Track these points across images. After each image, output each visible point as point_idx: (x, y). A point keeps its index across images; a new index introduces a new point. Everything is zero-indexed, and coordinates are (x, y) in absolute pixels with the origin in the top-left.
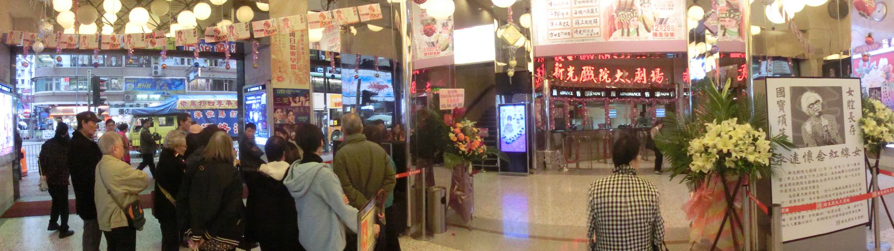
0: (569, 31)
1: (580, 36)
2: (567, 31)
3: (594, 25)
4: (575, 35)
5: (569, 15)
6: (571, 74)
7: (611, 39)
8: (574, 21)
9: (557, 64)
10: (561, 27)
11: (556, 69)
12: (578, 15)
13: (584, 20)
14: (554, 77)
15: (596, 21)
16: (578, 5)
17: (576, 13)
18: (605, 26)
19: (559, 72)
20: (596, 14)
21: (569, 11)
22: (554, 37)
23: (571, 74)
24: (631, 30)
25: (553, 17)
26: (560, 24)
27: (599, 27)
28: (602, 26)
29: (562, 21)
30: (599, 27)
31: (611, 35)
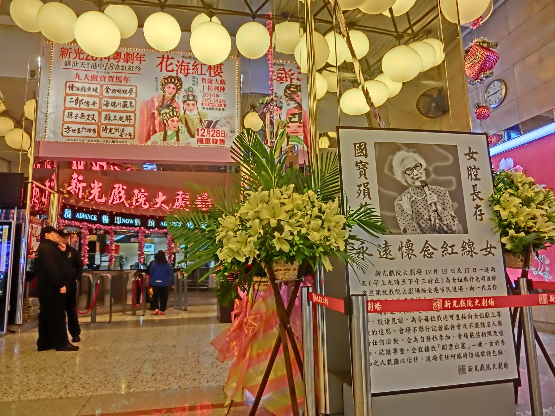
0: (96, 127)
1: (110, 135)
2: (92, 127)
3: (127, 123)
4: (103, 134)
5: (97, 105)
6: (95, 192)
7: (149, 143)
8: (103, 114)
9: (75, 176)
10: (83, 120)
11: (74, 182)
12: (110, 107)
13: (118, 115)
14: (69, 193)
15: (129, 118)
16: (111, 94)
17: (107, 105)
18: (142, 126)
19: (76, 186)
20: (130, 109)
21: (97, 100)
22: (71, 133)
23: (95, 192)
24: (169, 133)
25: (73, 105)
26: (83, 116)
27: (133, 126)
28: (137, 126)
29: (86, 113)
30: (133, 126)
31: (148, 138)
